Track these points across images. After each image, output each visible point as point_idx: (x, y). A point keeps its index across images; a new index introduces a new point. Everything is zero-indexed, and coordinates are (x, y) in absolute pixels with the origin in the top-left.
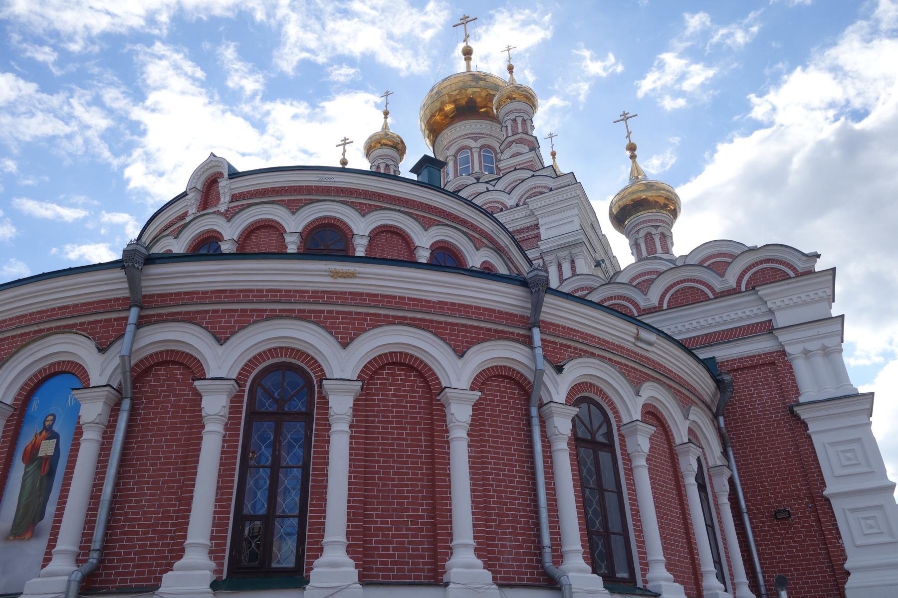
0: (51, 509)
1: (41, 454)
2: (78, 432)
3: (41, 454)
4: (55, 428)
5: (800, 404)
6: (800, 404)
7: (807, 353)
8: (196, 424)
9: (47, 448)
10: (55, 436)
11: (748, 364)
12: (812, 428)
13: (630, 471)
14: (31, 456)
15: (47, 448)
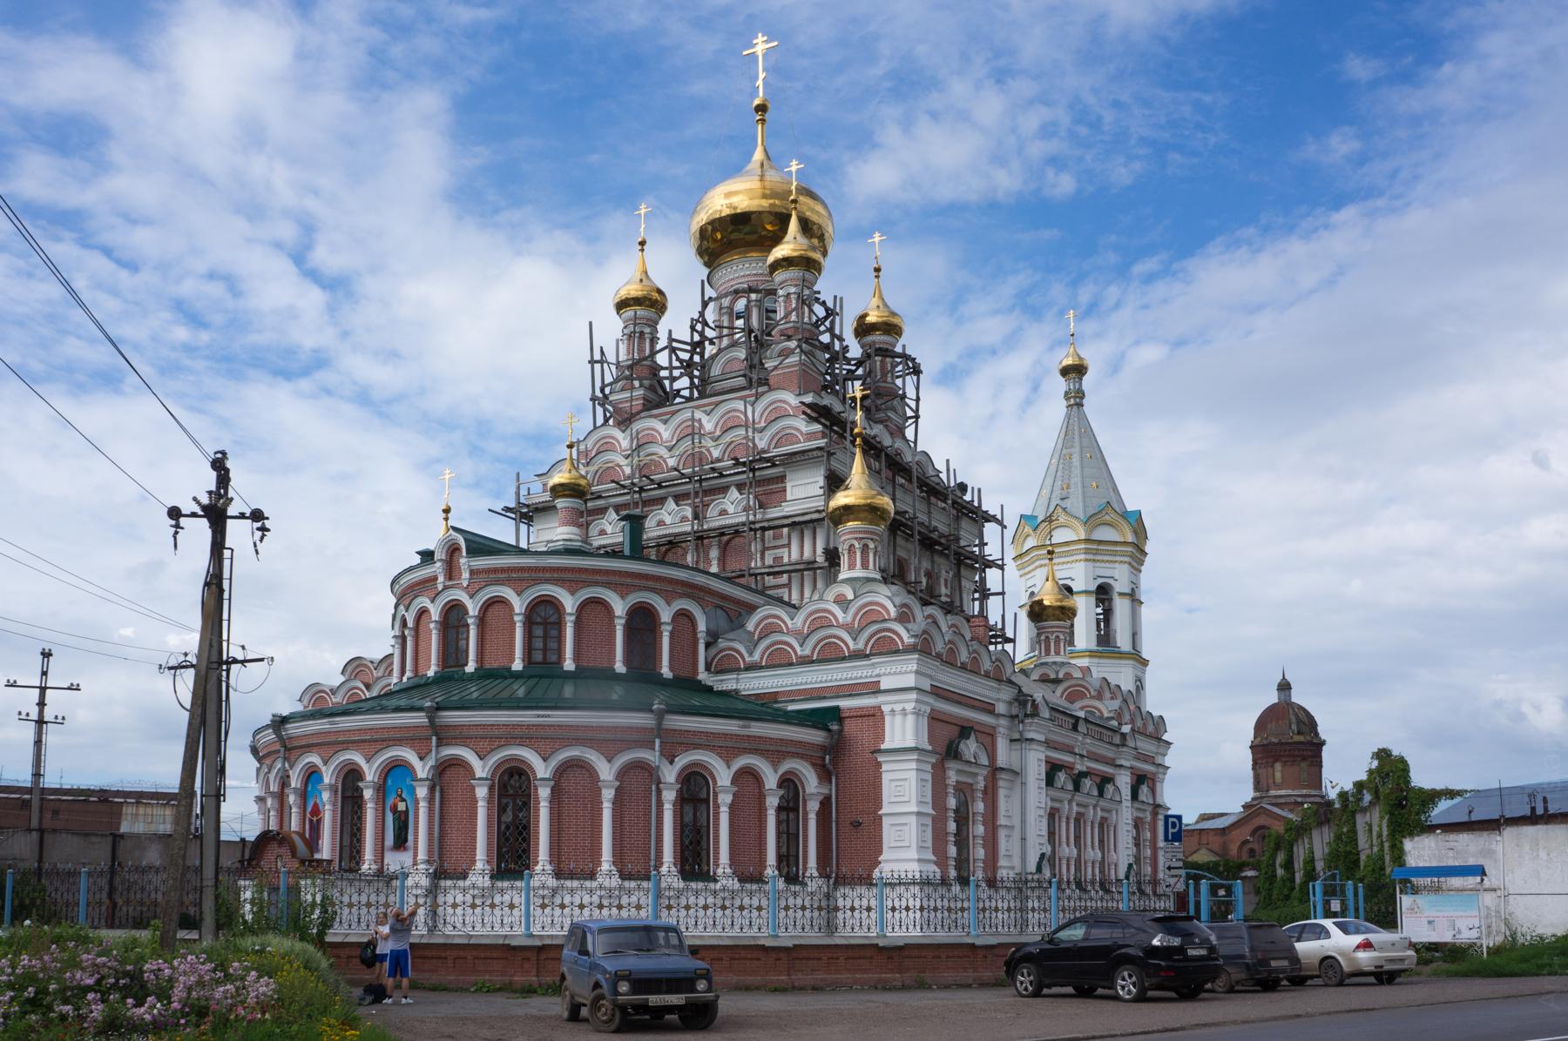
0: (410, 837)
1: (399, 809)
2: (417, 802)
3: (399, 809)
4: (404, 796)
5: (879, 751)
6: (879, 751)
7: (893, 711)
8: (474, 800)
9: (401, 807)
10: (403, 800)
11: (859, 714)
12: (885, 767)
13: (717, 814)
14: (394, 809)
15: (401, 807)
